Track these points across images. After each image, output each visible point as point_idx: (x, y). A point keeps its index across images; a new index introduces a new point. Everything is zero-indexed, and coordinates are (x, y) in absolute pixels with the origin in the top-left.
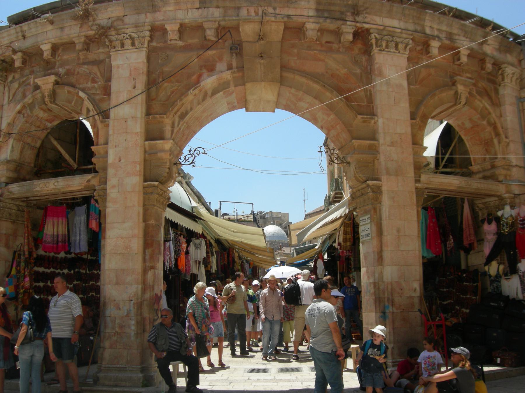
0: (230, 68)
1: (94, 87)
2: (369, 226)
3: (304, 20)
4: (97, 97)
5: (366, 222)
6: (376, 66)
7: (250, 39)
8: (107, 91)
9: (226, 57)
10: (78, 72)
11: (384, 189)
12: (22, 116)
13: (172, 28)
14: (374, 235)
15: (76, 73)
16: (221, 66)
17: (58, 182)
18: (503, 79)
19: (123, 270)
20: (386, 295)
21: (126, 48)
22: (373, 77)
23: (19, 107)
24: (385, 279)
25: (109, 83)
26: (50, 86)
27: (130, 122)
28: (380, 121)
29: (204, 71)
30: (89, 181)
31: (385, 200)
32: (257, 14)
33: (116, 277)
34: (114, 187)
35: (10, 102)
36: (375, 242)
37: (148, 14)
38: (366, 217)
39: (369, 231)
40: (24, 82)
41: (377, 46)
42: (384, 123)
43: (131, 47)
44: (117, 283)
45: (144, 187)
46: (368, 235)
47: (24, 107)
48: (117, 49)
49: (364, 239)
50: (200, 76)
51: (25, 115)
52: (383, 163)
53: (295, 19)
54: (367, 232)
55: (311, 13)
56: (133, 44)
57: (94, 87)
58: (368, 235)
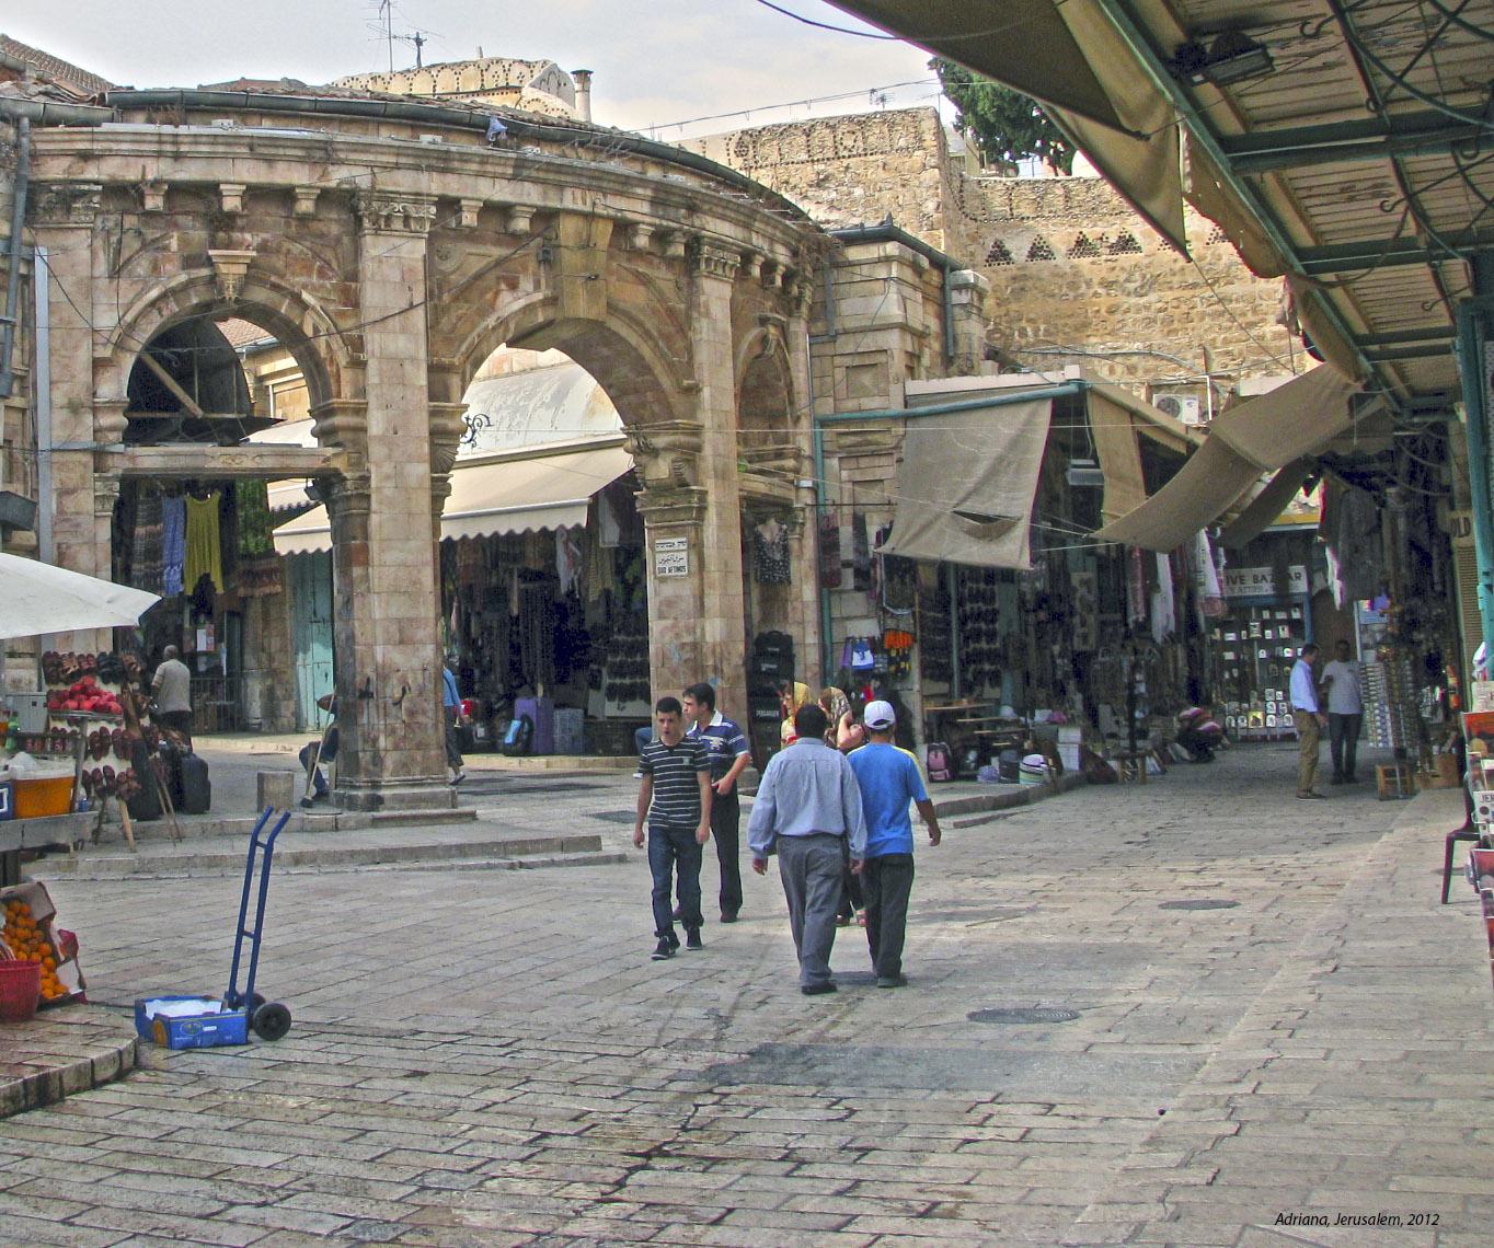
0: (537, 287)
1: (322, 286)
2: (684, 555)
3: (637, 217)
4: (332, 307)
6: (703, 298)
8: (352, 301)
9: (532, 265)
10: (289, 251)
11: (711, 498)
12: (155, 312)
14: (695, 568)
15: (284, 250)
16: (526, 284)
17: (261, 456)
18: (798, 307)
19: (411, 620)
20: (710, 663)
22: (695, 315)
23: (154, 293)
24: (708, 638)
26: (242, 270)
27: (408, 366)
28: (706, 392)
29: (503, 286)
30: (327, 460)
31: (711, 515)
32: (585, 203)
33: (401, 631)
34: (388, 477)
35: (115, 272)
36: (696, 581)
38: (675, 541)
39: (684, 563)
40: (154, 241)
41: (708, 265)
42: (712, 396)
44: (401, 642)
45: (433, 479)
47: (163, 296)
50: (497, 294)
51: (165, 313)
52: (710, 460)
53: (629, 216)
55: (646, 208)
57: (322, 286)
58: (679, 569)
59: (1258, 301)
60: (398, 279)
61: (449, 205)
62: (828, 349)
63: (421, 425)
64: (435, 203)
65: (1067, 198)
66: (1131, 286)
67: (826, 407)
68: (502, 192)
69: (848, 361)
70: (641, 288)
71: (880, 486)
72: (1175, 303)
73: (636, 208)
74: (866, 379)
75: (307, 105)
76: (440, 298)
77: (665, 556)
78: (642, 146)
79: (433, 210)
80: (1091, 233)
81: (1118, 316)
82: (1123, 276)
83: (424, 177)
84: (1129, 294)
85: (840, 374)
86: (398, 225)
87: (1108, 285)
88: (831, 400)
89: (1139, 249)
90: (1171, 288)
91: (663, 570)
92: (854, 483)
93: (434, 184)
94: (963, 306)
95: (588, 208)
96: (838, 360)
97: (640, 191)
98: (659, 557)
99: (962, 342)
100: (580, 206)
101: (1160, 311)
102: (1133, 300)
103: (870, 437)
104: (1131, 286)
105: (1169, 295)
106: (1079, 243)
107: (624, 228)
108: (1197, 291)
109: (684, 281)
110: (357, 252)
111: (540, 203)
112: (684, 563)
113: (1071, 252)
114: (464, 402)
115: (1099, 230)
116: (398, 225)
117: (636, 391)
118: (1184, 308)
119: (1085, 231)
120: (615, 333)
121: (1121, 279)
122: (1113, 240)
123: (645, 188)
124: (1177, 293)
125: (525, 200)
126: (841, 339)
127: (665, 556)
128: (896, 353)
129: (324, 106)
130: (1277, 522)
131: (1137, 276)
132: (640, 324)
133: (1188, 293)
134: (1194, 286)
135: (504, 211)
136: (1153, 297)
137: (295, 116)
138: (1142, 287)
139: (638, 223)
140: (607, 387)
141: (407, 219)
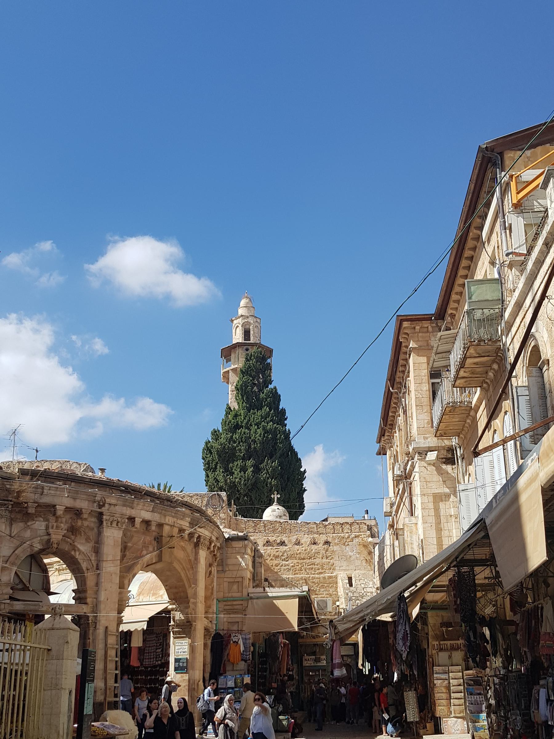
5: (183, 644)
7: (166, 536)
13: (138, 521)
21: (113, 526)
25: (97, 545)
27: (113, 576)
29: (144, 549)
37: (128, 508)
38: (183, 642)
43: (115, 526)
46: (184, 652)
48: (108, 525)
49: (179, 654)
54: (184, 650)
55: (188, 525)
56: (117, 525)
58: (184, 652)
59: (324, 565)
60: (113, 544)
61: (132, 520)
62: (222, 575)
63: (116, 598)
64: (127, 518)
65: (265, 527)
66: (283, 558)
67: (221, 595)
68: (147, 516)
69: (229, 580)
70: (183, 552)
71: (237, 625)
72: (297, 564)
73: (185, 524)
74: (235, 587)
75: (87, 480)
76: (124, 552)
77: (179, 647)
78: (187, 504)
79: (127, 520)
80: (271, 539)
81: (279, 567)
82: (281, 554)
83: (125, 508)
84: (282, 560)
85: (226, 584)
86: (114, 524)
87: (277, 557)
88: (222, 593)
89: (286, 546)
90: (296, 559)
91: (178, 652)
92: (228, 622)
93: (129, 512)
94: (261, 563)
95: (172, 524)
96: (225, 579)
97: (187, 519)
98: (177, 648)
99: (259, 574)
100: (170, 523)
101: (292, 566)
102: (284, 562)
103: (235, 607)
104: (283, 558)
105: (296, 561)
106: (267, 542)
107: (181, 531)
108: (305, 561)
109: (194, 550)
110: (100, 533)
111: (159, 521)
112: (186, 650)
113: (264, 545)
114: (129, 589)
115: (274, 538)
116: (114, 524)
117: (176, 587)
118: (300, 566)
119: (269, 538)
120: (174, 567)
121: (280, 555)
122: (278, 541)
123: (189, 518)
124: (299, 561)
125: (155, 519)
126: (228, 572)
127: (179, 647)
128: (246, 578)
129: (94, 481)
130: (350, 639)
131: (285, 554)
132: (182, 564)
133: (302, 561)
134: (304, 559)
135: (147, 523)
136: (290, 561)
137: (83, 483)
138: (287, 558)
139: (185, 530)
140: (165, 586)
141: (118, 522)
